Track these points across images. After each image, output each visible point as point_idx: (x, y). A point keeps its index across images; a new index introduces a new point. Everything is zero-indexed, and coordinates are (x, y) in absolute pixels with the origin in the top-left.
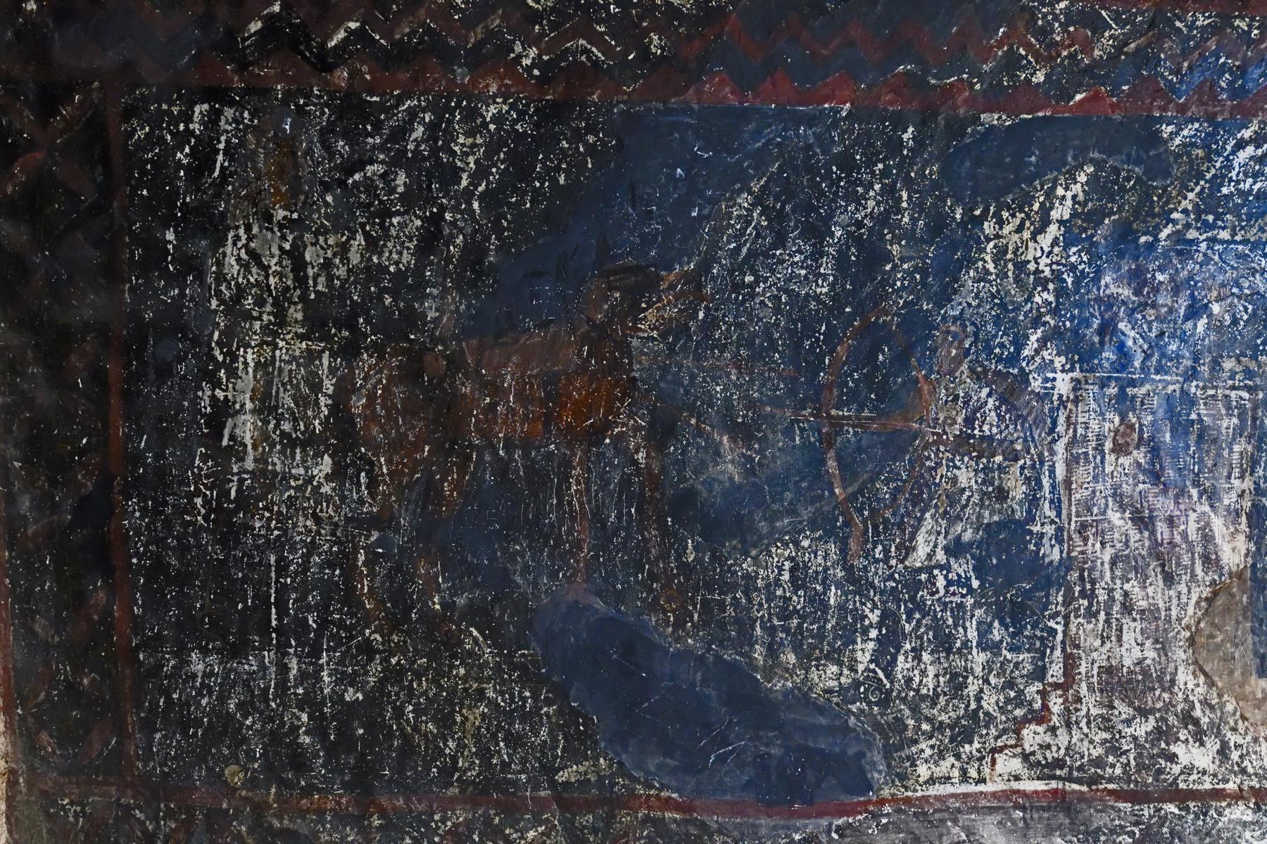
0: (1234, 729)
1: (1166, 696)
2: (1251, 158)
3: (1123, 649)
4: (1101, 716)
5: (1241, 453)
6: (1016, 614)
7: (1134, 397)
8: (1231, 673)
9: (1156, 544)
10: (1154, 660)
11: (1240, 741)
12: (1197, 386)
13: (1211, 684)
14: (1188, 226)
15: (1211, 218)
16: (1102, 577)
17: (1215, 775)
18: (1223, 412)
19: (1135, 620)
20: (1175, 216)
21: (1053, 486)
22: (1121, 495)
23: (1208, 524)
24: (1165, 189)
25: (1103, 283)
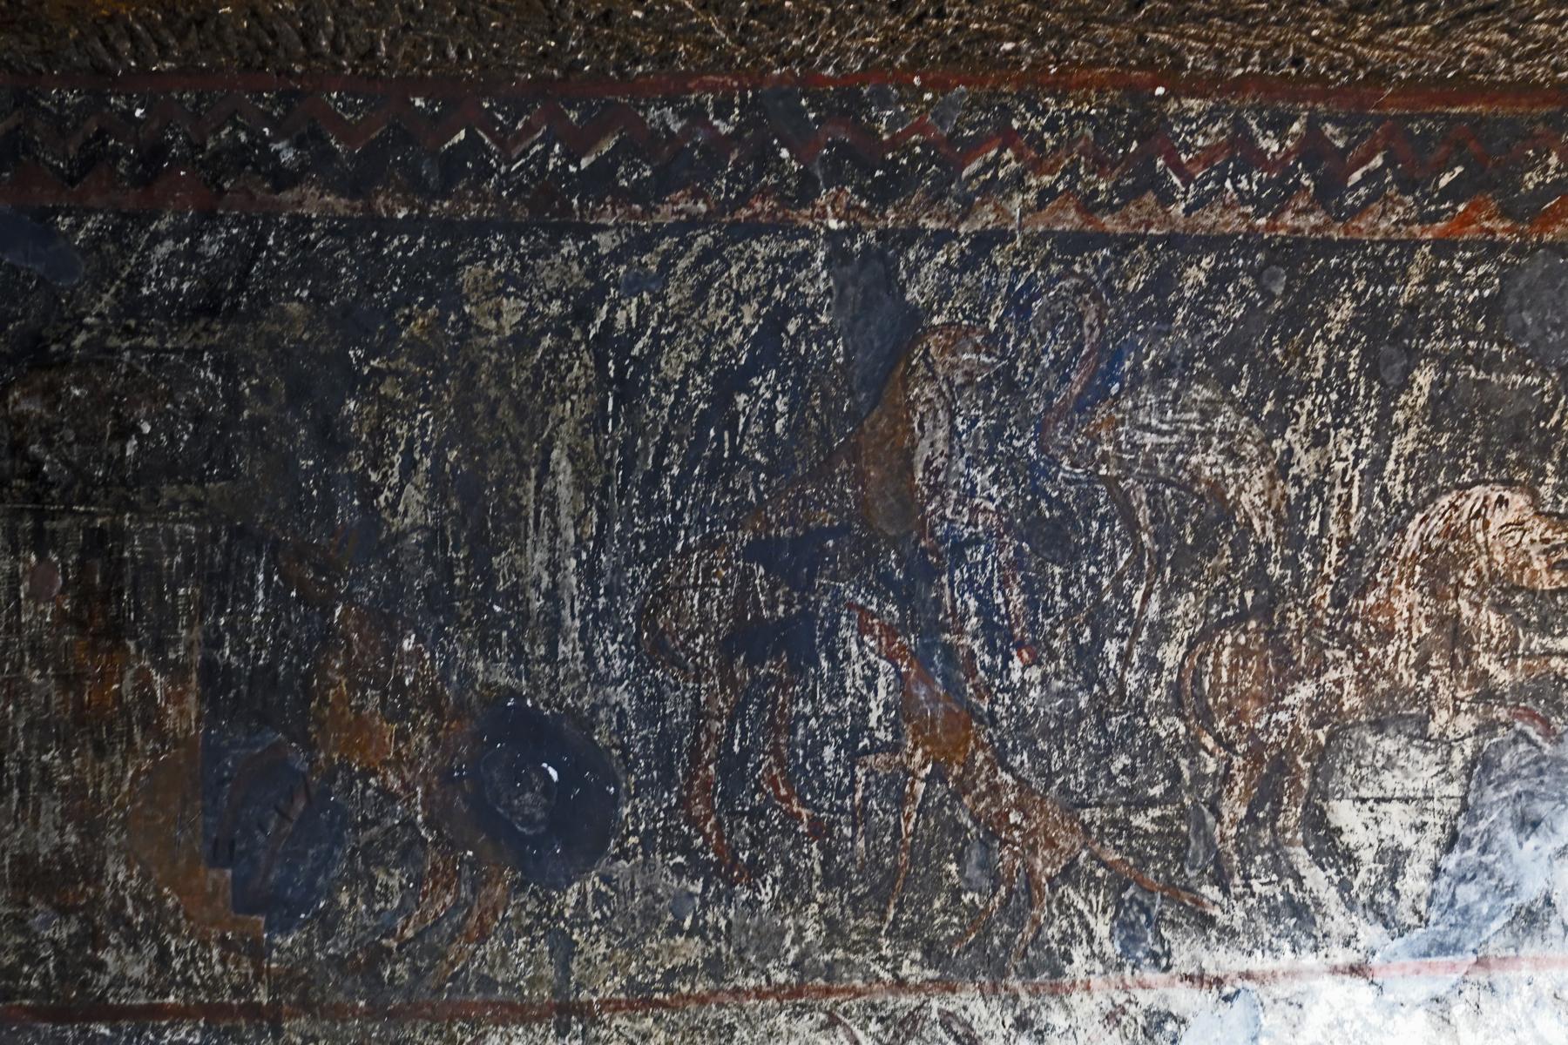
0: (176, 931)
1: (91, 890)
2: (172, 254)
3: (39, 835)
4: (14, 916)
5: (186, 595)
7: (54, 532)
9: (80, 706)
10: (75, 846)
11: (183, 945)
13: (145, 876)
14: (106, 332)
15: (132, 323)
16: (14, 746)
17: (150, 987)
18: (164, 548)
19: (55, 798)
20: (88, 320)
22: (41, 649)
23: (149, 681)
25: (11, 398)
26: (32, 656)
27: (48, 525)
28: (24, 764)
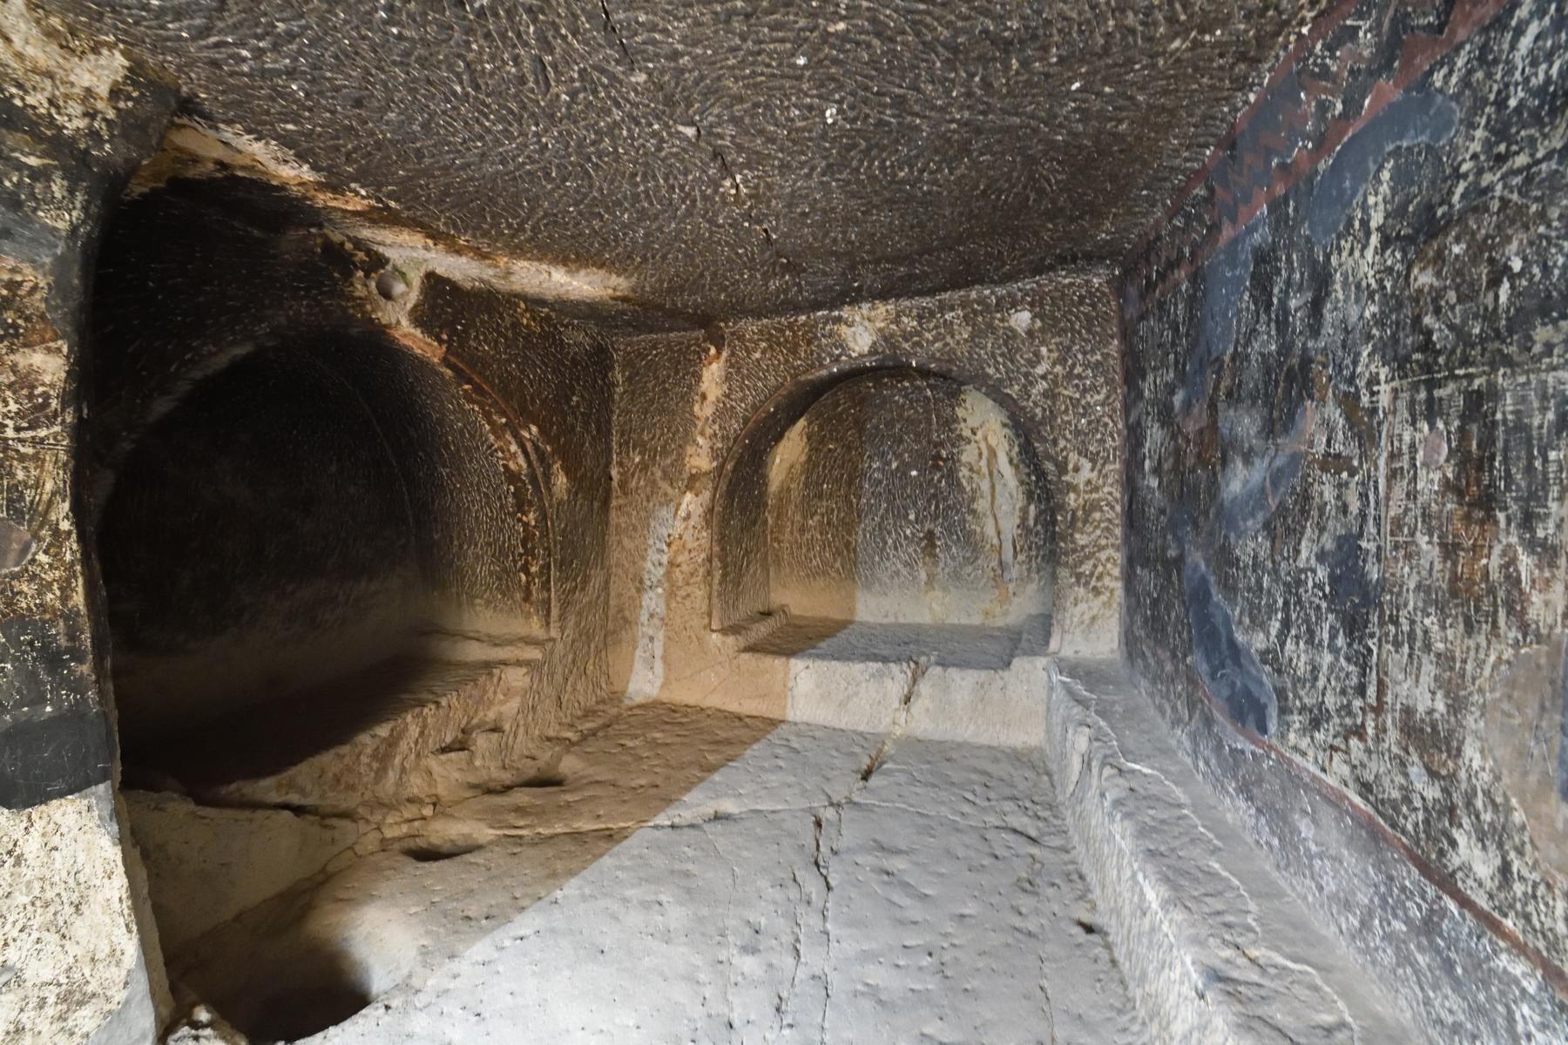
0: (1520, 852)
6: (1354, 626)
7: (1441, 399)
8: (1525, 774)
9: (1455, 578)
12: (1504, 375)
14: (1480, 172)
16: (1406, 605)
20: (1465, 168)
21: (1377, 503)
23: (1513, 561)
24: (1451, 142)
26: (1424, 521)
27: (1437, 393)
28: (1412, 622)
